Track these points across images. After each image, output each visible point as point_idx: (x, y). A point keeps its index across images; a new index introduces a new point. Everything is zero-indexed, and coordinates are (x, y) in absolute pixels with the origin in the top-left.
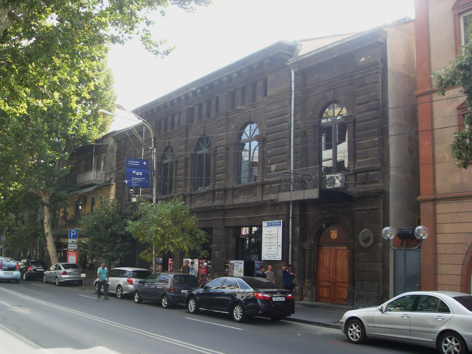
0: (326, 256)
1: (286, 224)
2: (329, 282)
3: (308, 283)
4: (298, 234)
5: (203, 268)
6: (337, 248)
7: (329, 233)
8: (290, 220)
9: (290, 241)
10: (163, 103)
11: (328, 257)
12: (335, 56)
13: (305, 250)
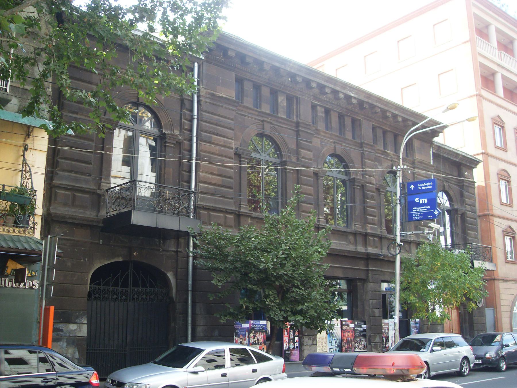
5: (349, 332)
10: (293, 71)
12: (457, 160)
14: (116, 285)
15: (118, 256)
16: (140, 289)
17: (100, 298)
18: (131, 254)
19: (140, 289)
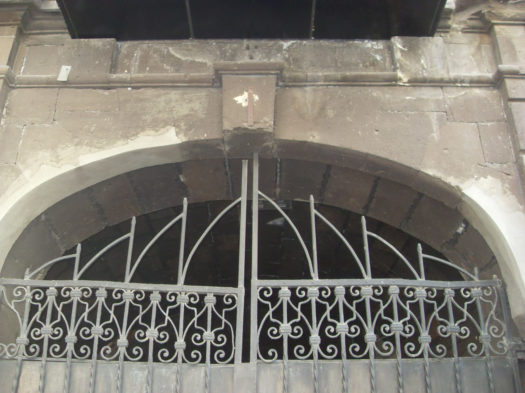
14: (157, 269)
15: (157, 125)
16: (313, 285)
17: (62, 343)
18: (218, 109)
19: (313, 285)
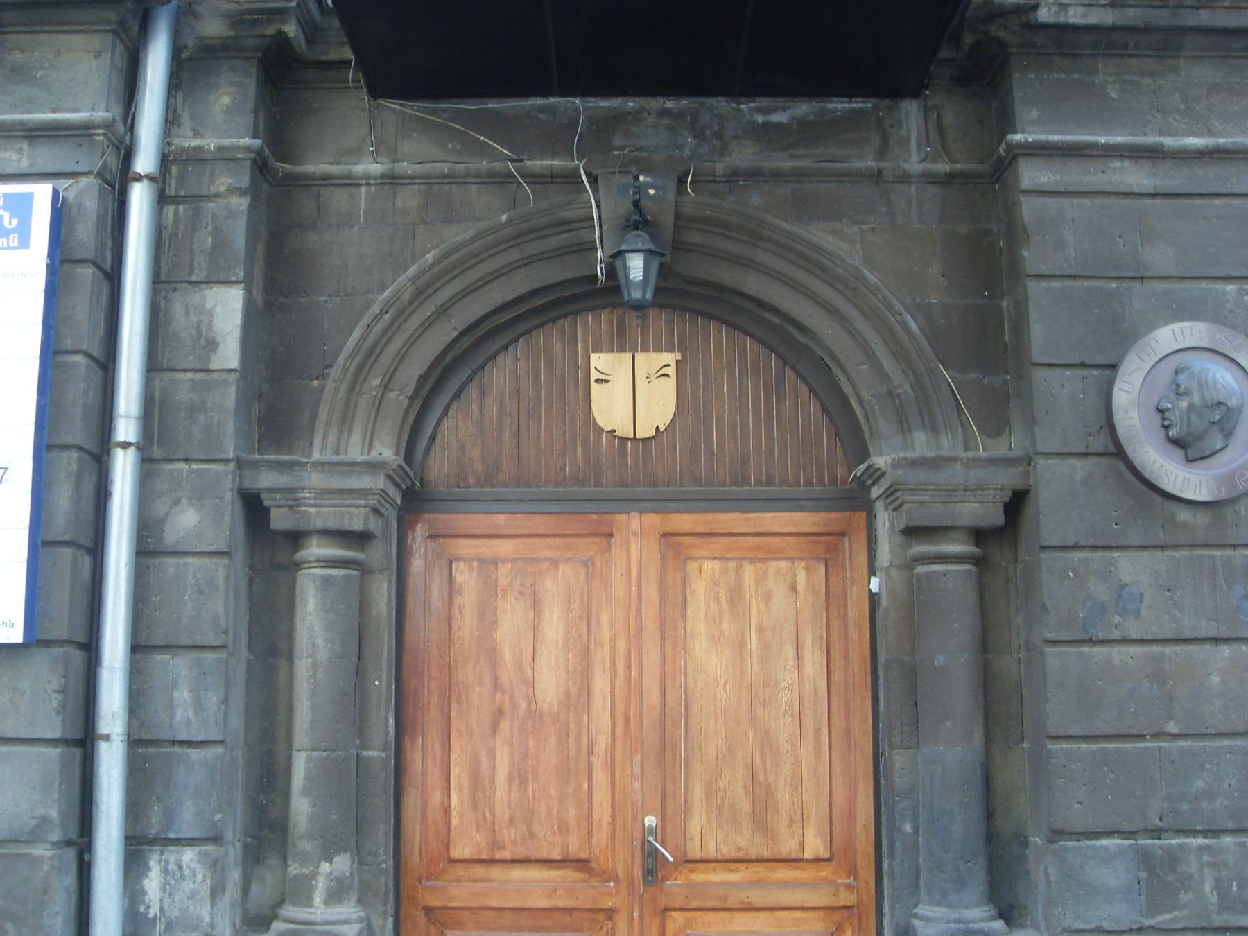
0: (536, 604)
1: (85, 232)
2: (581, 864)
3: (336, 894)
4: (229, 355)
6: (684, 521)
7: (579, 382)
8: (139, 198)
9: (126, 428)
11: (554, 625)
13: (296, 538)
